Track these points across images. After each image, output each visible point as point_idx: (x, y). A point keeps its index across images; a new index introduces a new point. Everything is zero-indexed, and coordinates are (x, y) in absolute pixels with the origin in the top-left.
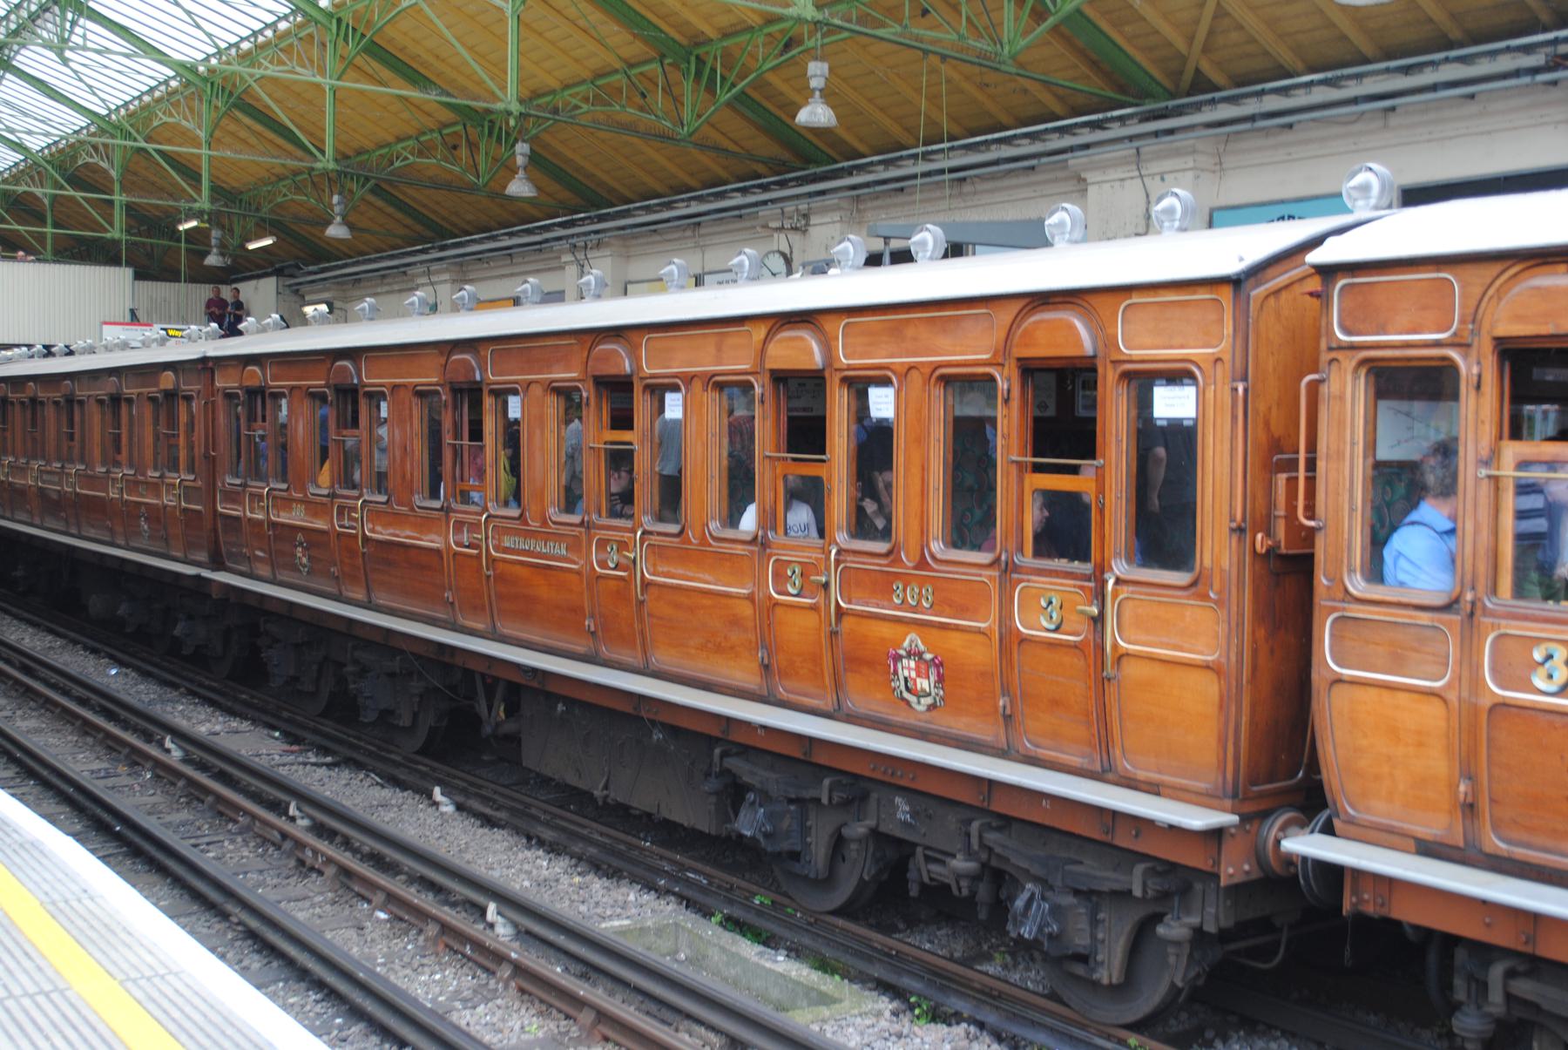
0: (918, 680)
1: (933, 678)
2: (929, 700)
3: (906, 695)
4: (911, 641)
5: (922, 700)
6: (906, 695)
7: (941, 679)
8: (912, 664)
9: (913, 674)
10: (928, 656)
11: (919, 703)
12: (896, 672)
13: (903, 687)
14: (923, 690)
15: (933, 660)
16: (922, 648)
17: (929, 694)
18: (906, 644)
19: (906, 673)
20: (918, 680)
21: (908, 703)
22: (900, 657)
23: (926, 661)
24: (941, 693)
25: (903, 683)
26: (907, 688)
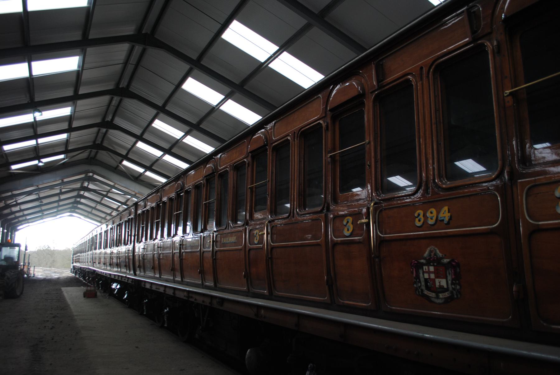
0: (437, 280)
1: (449, 278)
2: (447, 294)
3: (426, 292)
4: (431, 252)
5: (441, 295)
6: (426, 292)
7: (457, 278)
8: (432, 269)
9: (432, 276)
10: (446, 261)
11: (438, 297)
12: (418, 277)
13: (423, 288)
14: (441, 287)
15: (449, 262)
16: (440, 255)
17: (447, 290)
18: (426, 254)
19: (426, 276)
20: (437, 280)
21: (428, 298)
22: (422, 265)
23: (444, 265)
24: (458, 287)
25: (423, 283)
26: (428, 288)
